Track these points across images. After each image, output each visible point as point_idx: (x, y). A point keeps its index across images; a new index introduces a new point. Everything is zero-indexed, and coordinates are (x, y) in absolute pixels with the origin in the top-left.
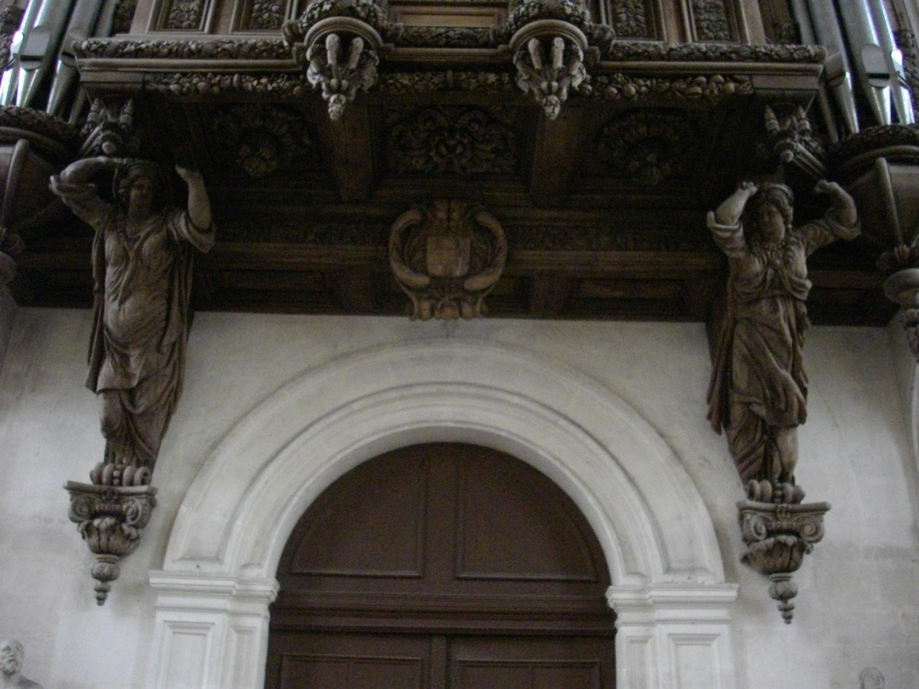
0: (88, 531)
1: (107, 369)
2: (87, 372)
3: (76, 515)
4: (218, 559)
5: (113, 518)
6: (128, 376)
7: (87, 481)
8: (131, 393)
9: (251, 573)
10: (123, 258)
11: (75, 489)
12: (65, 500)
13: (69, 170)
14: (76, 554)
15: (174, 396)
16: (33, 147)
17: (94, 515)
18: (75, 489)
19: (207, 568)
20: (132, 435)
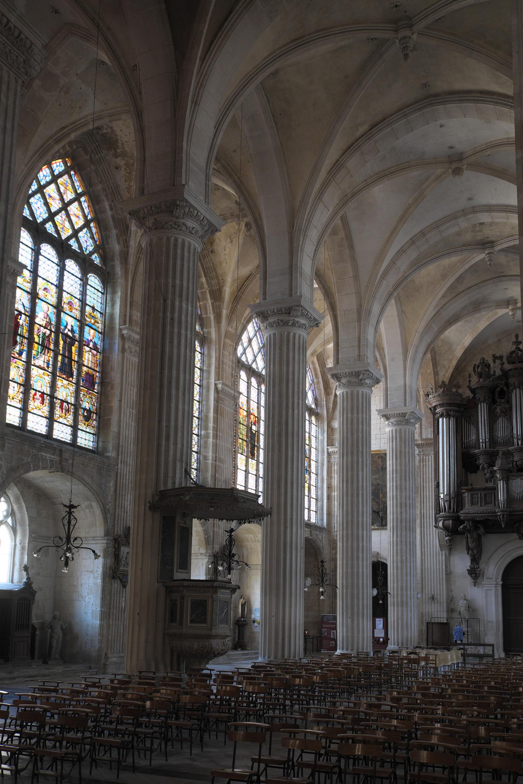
0: (471, 576)
1: (470, 552)
2: (466, 552)
3: (469, 574)
4: (492, 579)
5: (475, 574)
6: (474, 552)
7: (469, 568)
8: (475, 555)
9: (498, 580)
10: (471, 538)
11: (468, 570)
12: (467, 572)
13: (461, 527)
14: (469, 580)
15: (481, 554)
16: (452, 520)
17: (472, 574)
18: (468, 570)
19: (491, 580)
20: (475, 560)
